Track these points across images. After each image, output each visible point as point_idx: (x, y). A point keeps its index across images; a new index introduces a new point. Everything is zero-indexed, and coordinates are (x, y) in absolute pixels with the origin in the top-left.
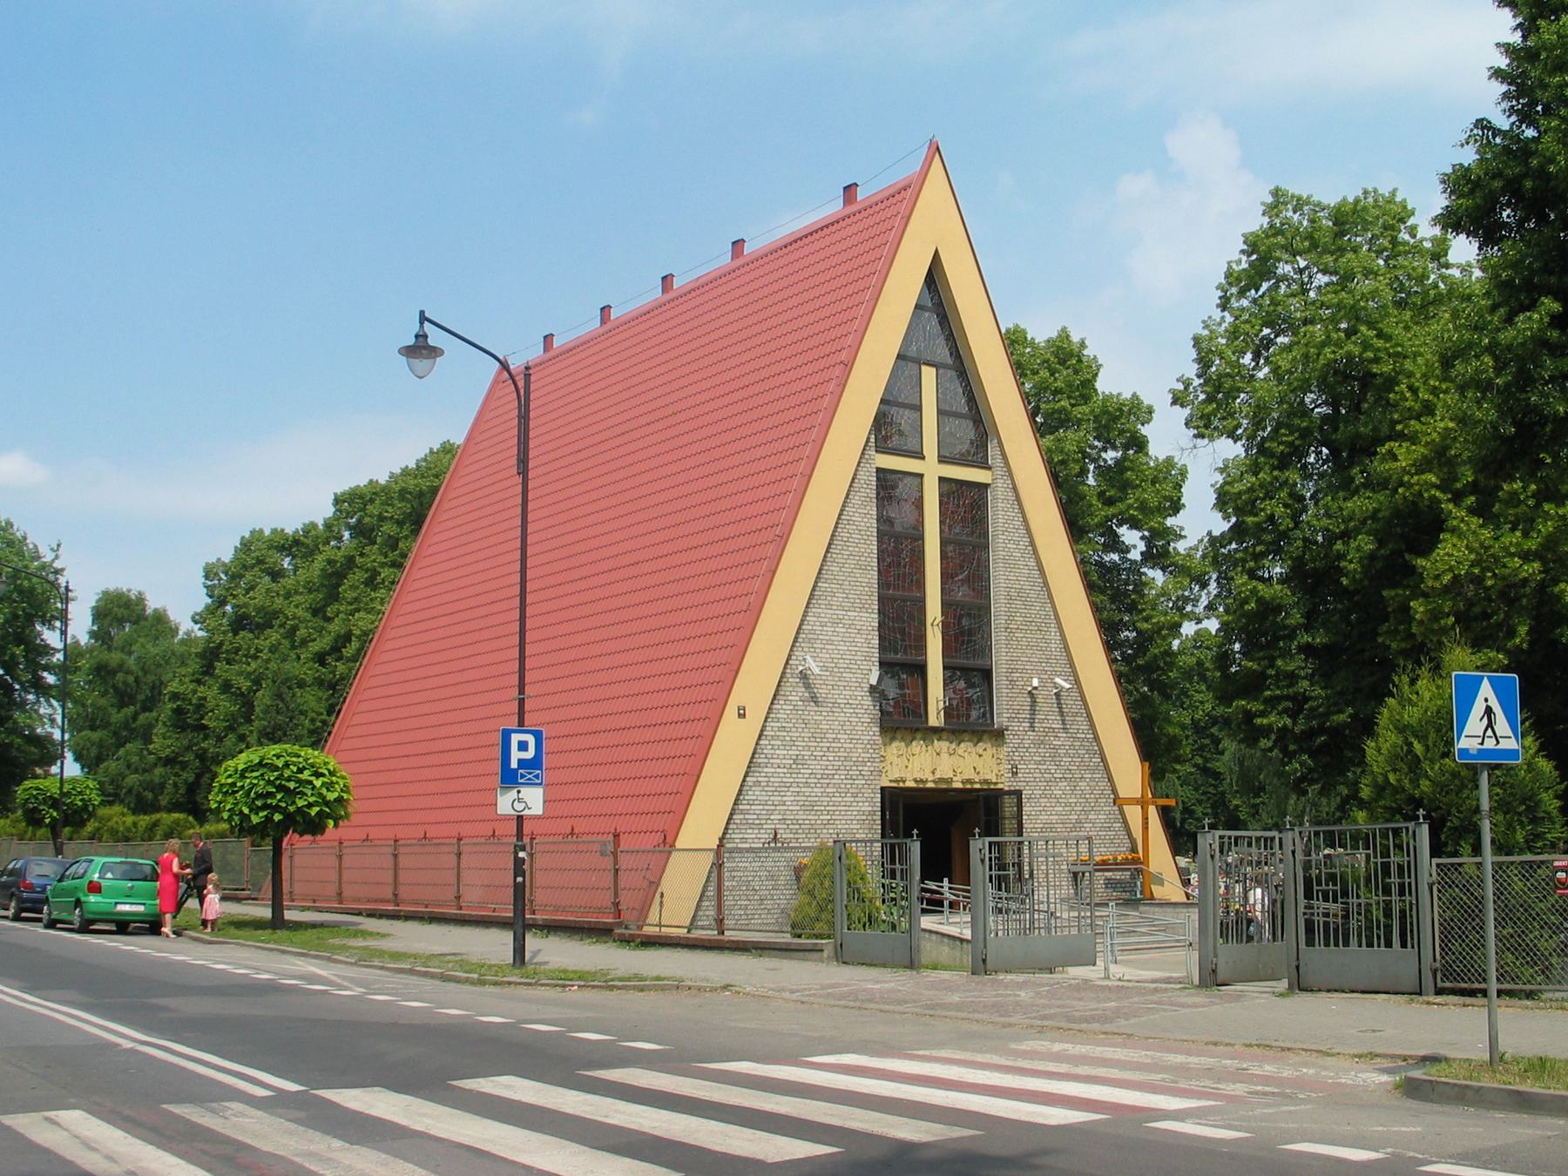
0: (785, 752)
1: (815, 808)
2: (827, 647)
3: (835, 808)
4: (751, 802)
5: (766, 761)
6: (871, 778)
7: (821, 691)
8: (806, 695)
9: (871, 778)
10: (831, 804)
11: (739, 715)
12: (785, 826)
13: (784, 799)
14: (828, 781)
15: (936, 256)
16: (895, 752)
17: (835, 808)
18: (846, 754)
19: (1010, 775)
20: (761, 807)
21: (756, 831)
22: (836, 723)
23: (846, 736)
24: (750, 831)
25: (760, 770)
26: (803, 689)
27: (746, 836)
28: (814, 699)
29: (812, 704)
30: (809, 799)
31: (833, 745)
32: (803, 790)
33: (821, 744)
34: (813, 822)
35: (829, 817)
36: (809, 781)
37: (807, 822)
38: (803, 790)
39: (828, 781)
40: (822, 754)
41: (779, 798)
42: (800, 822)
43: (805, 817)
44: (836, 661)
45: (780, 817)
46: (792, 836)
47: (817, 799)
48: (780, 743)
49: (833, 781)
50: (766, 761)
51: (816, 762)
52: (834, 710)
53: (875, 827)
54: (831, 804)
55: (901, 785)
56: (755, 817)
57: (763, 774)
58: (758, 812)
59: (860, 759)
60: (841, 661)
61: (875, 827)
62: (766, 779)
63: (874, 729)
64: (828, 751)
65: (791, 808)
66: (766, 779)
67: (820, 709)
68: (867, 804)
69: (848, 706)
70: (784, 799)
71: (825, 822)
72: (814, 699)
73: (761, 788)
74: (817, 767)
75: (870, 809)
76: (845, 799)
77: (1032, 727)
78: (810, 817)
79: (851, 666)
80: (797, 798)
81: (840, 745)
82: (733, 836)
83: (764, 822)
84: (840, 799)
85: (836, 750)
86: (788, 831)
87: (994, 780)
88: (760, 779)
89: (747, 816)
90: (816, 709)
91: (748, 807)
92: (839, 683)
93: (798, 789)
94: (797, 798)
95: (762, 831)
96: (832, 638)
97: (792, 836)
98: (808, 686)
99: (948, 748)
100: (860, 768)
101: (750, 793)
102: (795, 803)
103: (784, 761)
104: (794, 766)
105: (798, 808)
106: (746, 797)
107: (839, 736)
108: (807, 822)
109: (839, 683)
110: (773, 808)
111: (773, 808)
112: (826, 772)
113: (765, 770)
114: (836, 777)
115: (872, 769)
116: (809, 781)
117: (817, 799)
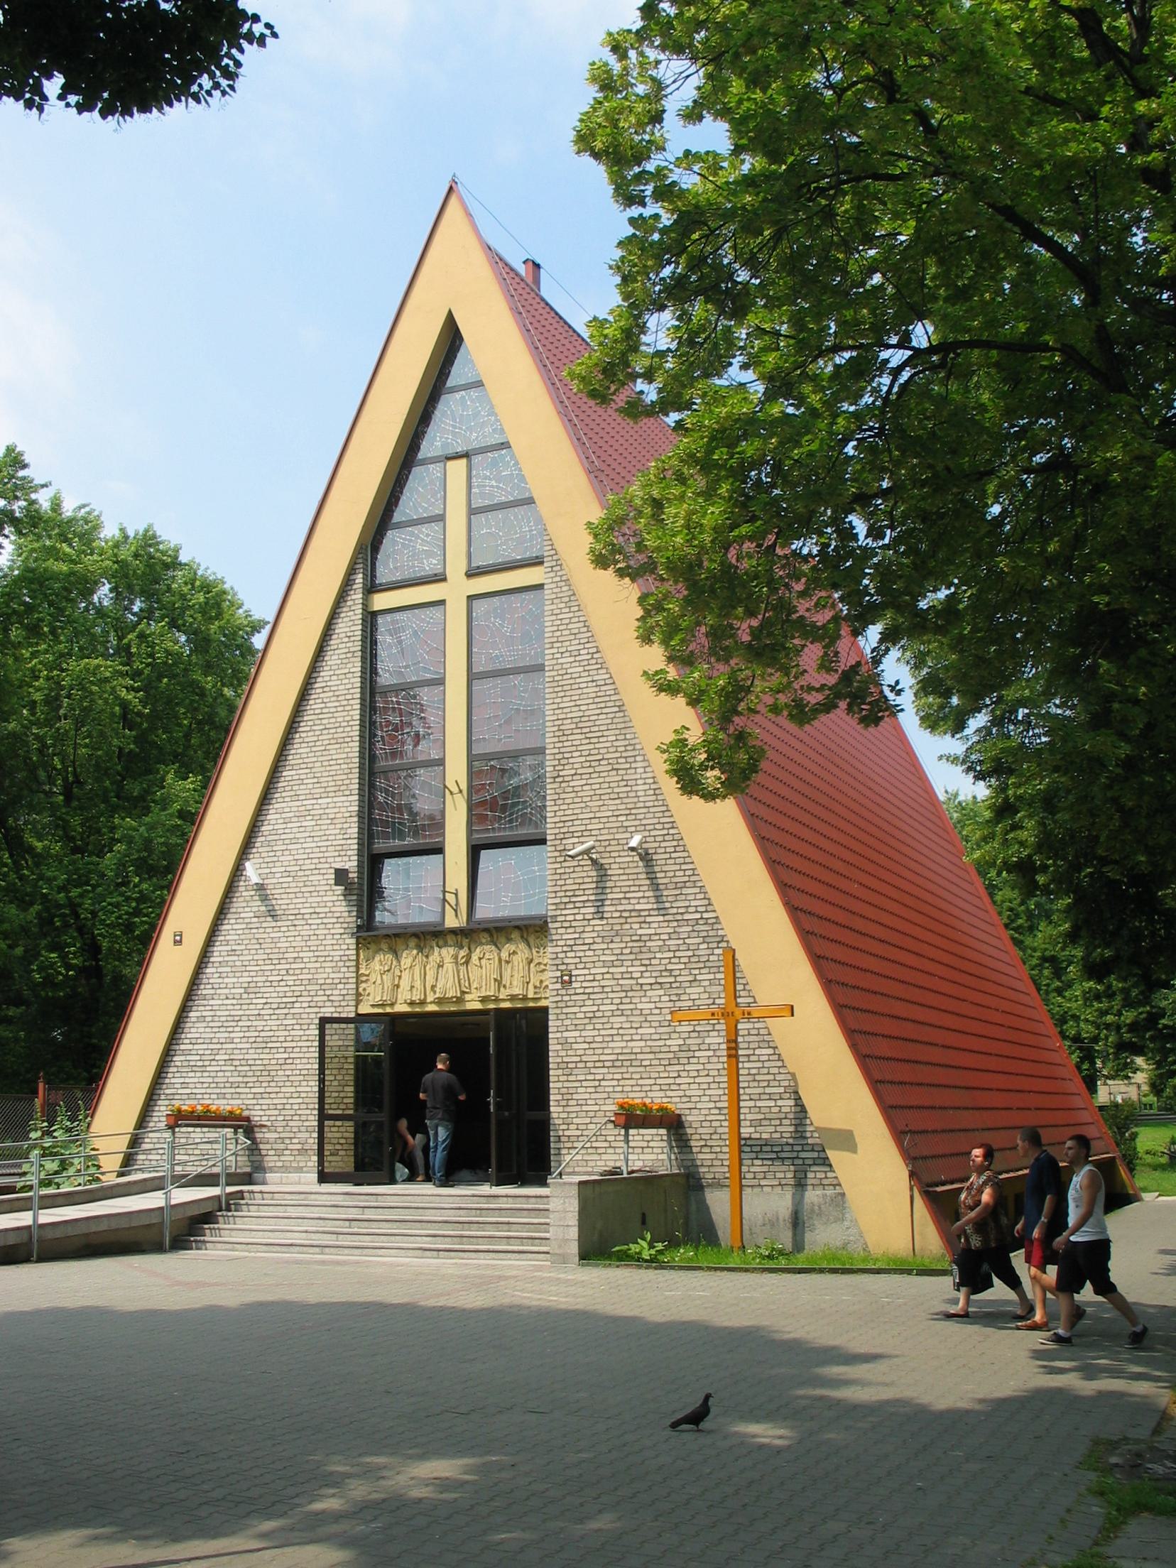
0: (235, 980)
1: (270, 1045)
2: (290, 847)
3: (294, 1044)
4: (194, 1041)
5: (212, 992)
6: (343, 1004)
7: (281, 903)
8: (263, 908)
9: (343, 1004)
10: (289, 1039)
11: (181, 936)
12: (233, 1068)
13: (232, 1035)
14: (286, 1011)
15: (450, 313)
16: (377, 968)
17: (294, 1044)
18: (310, 976)
19: (559, 986)
20: (205, 1046)
21: (199, 1074)
22: (299, 938)
23: (311, 954)
24: (192, 1074)
25: (205, 1002)
26: (259, 903)
27: (187, 1080)
28: (272, 914)
29: (269, 919)
30: (262, 1034)
31: (293, 966)
32: (255, 1023)
33: (278, 967)
34: (265, 1062)
35: (286, 1056)
36: (262, 1012)
37: (258, 1062)
38: (255, 1023)
39: (286, 1011)
40: (280, 978)
41: (226, 1035)
42: (250, 1062)
43: (256, 1056)
44: (300, 862)
45: (227, 1057)
46: (240, 1079)
47: (271, 1034)
48: (228, 969)
49: (292, 1011)
50: (212, 992)
51: (272, 989)
52: (296, 922)
53: (346, 1066)
54: (289, 1039)
55: (388, 1010)
56: (198, 1057)
57: (208, 1008)
58: (200, 1052)
59: (328, 981)
60: (308, 862)
61: (346, 1066)
62: (212, 1013)
63: (348, 941)
64: (288, 974)
65: (239, 1046)
66: (212, 1013)
67: (279, 924)
68: (336, 1037)
69: (314, 916)
70: (232, 1035)
71: (281, 1062)
72: (272, 914)
73: (204, 1024)
74: (272, 995)
75: (340, 1043)
76: (307, 1032)
77: (600, 914)
78: (262, 1056)
79: (319, 866)
80: (247, 1034)
81: (302, 965)
82: (173, 1081)
83: (207, 1063)
84: (301, 1033)
85: (298, 972)
86: (236, 1074)
87: (531, 995)
88: (204, 1014)
89: (189, 1058)
90: (274, 924)
91: (190, 1047)
92: (303, 889)
93: (249, 1023)
94: (247, 1034)
95: (206, 1074)
96: (298, 835)
97: (240, 1079)
98: (265, 899)
99: (456, 957)
100: (328, 992)
101: (192, 1030)
102: (244, 1040)
103: (233, 991)
104: (245, 996)
105: (248, 1046)
106: (189, 1036)
107: (301, 955)
108: (258, 1062)
109: (303, 889)
110: (219, 1046)
111: (219, 1046)
112: (285, 1000)
113: (211, 1002)
114: (297, 1005)
115: (345, 992)
116: (262, 1012)
117: (271, 1034)
